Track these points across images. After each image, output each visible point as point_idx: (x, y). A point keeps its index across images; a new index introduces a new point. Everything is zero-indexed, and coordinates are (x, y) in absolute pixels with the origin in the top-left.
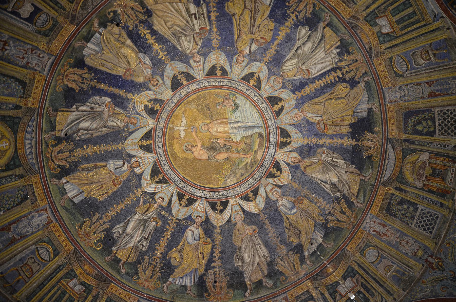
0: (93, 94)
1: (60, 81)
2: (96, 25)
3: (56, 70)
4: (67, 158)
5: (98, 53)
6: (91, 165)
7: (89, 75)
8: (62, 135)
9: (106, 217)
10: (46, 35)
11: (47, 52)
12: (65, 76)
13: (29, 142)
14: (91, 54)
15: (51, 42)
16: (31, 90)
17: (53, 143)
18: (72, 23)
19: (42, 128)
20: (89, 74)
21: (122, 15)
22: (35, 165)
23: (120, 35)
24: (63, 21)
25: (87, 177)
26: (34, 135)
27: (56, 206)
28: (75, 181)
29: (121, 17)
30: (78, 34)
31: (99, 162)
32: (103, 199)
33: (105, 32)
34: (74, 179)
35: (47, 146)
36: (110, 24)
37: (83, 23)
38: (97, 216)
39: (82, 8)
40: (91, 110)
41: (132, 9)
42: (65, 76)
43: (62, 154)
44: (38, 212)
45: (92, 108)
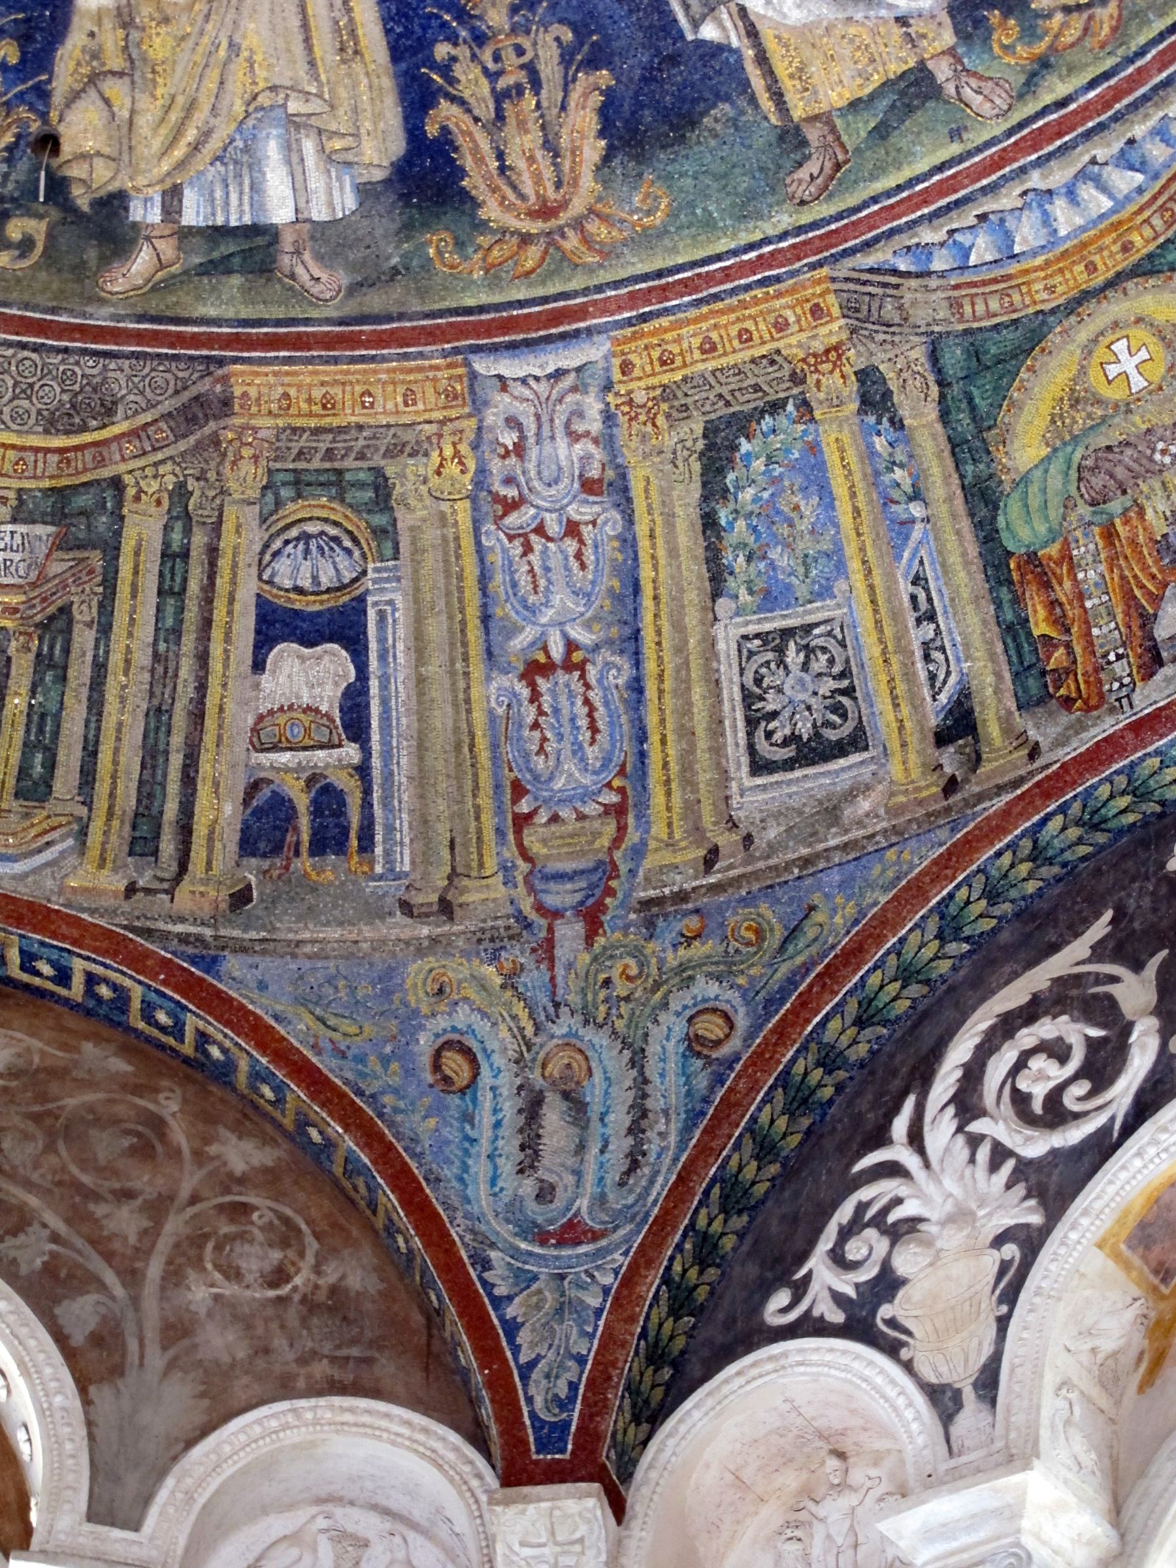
2: (141, 263)
3: (545, 300)
5: (294, 123)
7: (458, 71)
11: (473, 423)
13: (1059, 208)
14: (328, 158)
15: (409, 436)
18: (227, 402)
19: (940, 168)
20: (452, 81)
23: (93, 79)
24: (247, 452)
26: (1008, 199)
33: (141, 181)
35: (1044, 64)
36: (77, 191)
39: (108, 411)
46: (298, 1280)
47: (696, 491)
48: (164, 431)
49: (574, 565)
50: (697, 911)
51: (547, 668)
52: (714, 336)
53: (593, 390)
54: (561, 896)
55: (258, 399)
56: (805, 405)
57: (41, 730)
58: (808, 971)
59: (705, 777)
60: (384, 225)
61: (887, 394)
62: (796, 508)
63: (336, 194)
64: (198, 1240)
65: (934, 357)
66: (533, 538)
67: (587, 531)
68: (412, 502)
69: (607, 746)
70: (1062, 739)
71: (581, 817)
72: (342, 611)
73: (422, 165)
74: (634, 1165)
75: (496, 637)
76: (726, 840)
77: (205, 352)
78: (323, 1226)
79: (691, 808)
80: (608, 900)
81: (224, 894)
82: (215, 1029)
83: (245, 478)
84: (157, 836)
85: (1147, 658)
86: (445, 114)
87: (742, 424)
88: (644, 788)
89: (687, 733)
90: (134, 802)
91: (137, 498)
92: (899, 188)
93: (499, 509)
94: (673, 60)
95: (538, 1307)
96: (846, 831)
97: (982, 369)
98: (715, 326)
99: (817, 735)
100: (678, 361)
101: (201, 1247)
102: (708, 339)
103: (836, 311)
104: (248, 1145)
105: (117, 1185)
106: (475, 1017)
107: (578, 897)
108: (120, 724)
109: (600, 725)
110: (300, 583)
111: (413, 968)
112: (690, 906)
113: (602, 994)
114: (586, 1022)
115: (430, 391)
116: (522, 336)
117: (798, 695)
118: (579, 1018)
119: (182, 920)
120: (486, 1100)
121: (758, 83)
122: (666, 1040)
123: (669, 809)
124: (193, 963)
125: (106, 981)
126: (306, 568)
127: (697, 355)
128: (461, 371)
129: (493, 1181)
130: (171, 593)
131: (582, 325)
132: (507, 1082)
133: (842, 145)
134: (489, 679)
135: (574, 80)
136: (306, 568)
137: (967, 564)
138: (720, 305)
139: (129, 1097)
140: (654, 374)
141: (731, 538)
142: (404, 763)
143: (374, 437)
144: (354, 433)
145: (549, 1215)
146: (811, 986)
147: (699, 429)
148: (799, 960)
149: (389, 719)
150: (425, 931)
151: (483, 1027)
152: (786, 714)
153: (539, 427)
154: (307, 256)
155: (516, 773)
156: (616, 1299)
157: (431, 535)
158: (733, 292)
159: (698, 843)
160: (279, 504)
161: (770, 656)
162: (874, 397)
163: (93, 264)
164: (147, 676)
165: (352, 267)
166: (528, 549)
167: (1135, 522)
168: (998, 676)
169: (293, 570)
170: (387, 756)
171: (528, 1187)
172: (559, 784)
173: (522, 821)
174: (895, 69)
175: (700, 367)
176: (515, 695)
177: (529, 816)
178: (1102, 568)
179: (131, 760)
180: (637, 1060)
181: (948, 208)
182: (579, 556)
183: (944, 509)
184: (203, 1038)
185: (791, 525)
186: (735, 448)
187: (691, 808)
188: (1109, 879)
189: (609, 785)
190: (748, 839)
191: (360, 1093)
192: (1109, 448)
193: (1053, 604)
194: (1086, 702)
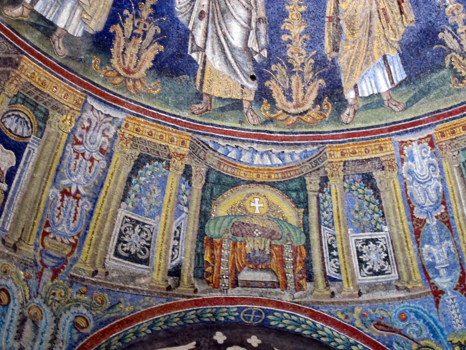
0: (171, 11)
1: (139, 87)
2: (17, 11)
3: (115, 94)
4: (303, 81)
6: (328, 29)
7: (127, 20)
8: (253, 86)
9: (454, 15)
10: (45, 118)
11: (79, 114)
12: (128, 76)
13: (257, 156)
14: (81, 18)
15: (61, 107)
16: (155, 144)
17: (266, 106)
18: (17, 65)
20: (124, 22)
22: (306, 151)
24: (15, 82)
25: (353, 42)
26: (245, 146)
27: (400, 122)
28: (357, 71)
31: (325, 8)
32: (412, 12)
34: (352, 71)
35: (271, 120)
38: (446, 36)
40: (205, 19)
42: (128, 76)
43: (294, 92)
44: (402, 160)
45: (201, 15)
47: (129, 170)
49: (88, 170)
50: (86, 286)
51: (69, 194)
52: (154, 132)
54: (49, 262)
55: (26, 70)
56: (168, 165)
58: (114, 320)
59: (101, 249)
60: (85, 45)
61: (191, 175)
62: (154, 190)
63: (78, 29)
65: (208, 173)
66: (80, 155)
67: (95, 162)
68: (52, 125)
69: (77, 226)
70: (204, 292)
71: (62, 242)
73: (103, 37)
75: (58, 177)
76: (100, 270)
77: (19, 47)
79: (94, 256)
80: (62, 270)
85: (234, 282)
86: (117, 28)
87: (150, 159)
89: (100, 234)
92: (220, 126)
93: (75, 142)
94: (181, 56)
96: (136, 285)
97: (219, 184)
98: (155, 130)
99: (136, 254)
100: (141, 133)
102: (151, 132)
103: (188, 146)
106: (13, 285)
107: (54, 264)
109: (77, 218)
110: (11, 128)
114: (45, 303)
115: (72, 98)
116: (104, 99)
117: (134, 241)
121: (199, 77)
122: (67, 319)
123: (88, 253)
126: (15, 125)
127: (146, 134)
128: (84, 98)
129: (7, 338)
131: (121, 107)
132: (17, 309)
133: (211, 106)
134: (51, 188)
135: (154, 43)
136: (15, 125)
137: (193, 231)
138: (159, 125)
142: (18, 198)
143: (51, 101)
144: (46, 96)
146: (115, 325)
147: (138, 153)
148: (113, 315)
149: (19, 183)
150: (7, 251)
151: (14, 289)
152: (129, 244)
153: (96, 126)
154: (61, 40)
155: (48, 219)
157: (53, 137)
158: (165, 124)
160: (16, 102)
161: (131, 226)
162: (187, 173)
165: (71, 51)
166: (77, 158)
167: (243, 246)
168: (191, 266)
170: (14, 193)
172: (60, 229)
173: (45, 234)
174: (234, 96)
176: (57, 197)
178: (230, 252)
180: (57, 321)
181: (229, 139)
182: (90, 168)
183: (193, 213)
185: (151, 194)
186: (145, 164)
187: (94, 256)
188: (195, 333)
189: (73, 237)
190: (107, 273)
192: (243, 223)
193: (212, 254)
194: (214, 285)
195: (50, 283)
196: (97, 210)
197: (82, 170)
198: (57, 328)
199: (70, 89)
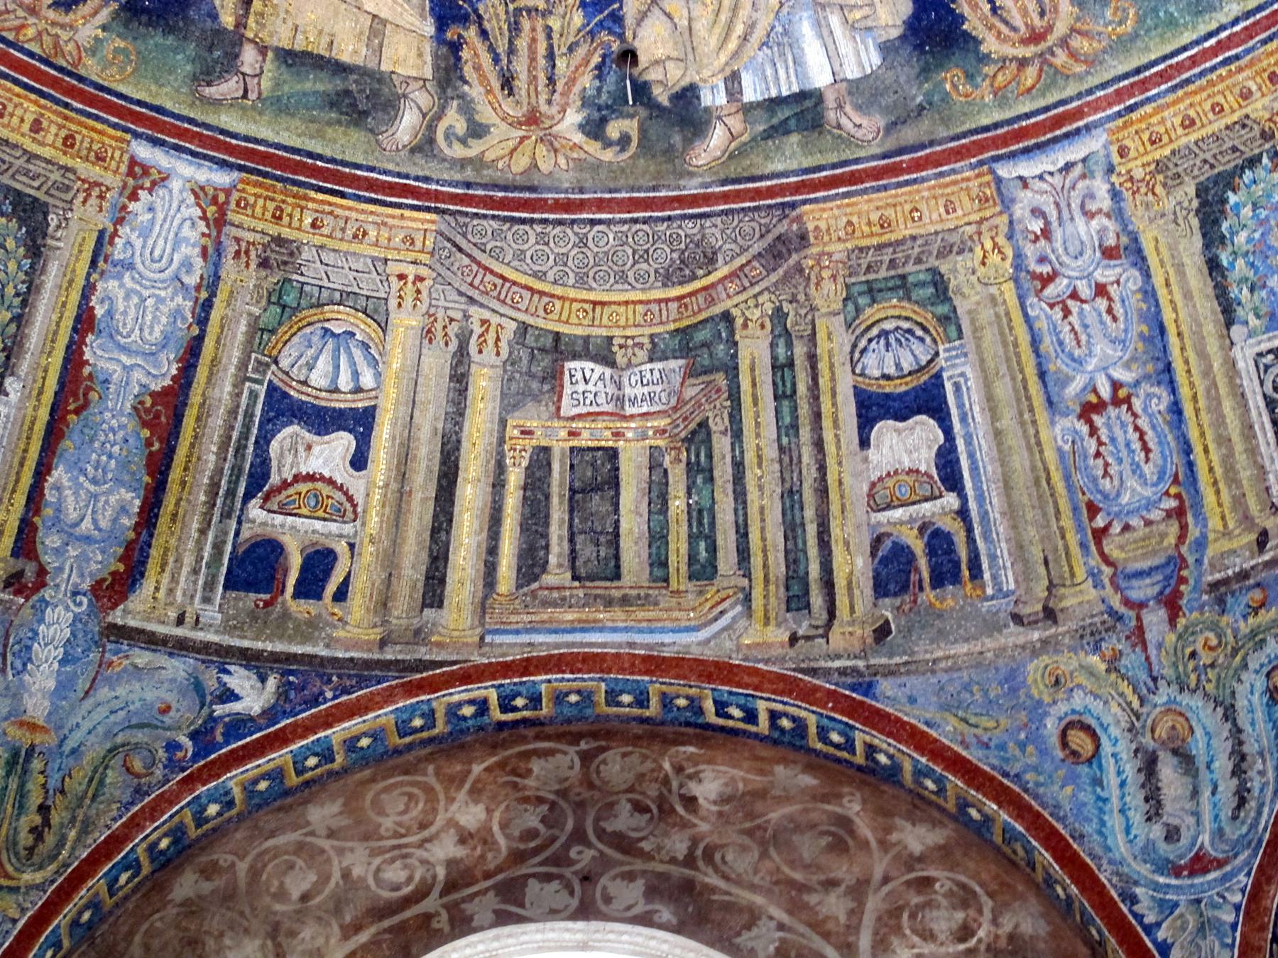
2: (717, 139)
3: (1047, 109)
11: (1004, 219)
14: (852, 27)
15: (954, 238)
16: (1217, 138)
18: (803, 237)
21: (577, 89)
29: (587, 81)
30: (820, 168)
33: (706, 73)
37: (758, 194)
39: (710, 260)
41: (508, 83)
42: (1043, 46)
46: (981, 933)
48: (757, 269)
49: (1108, 319)
50: (1258, 585)
51: (1099, 407)
52: (1192, 113)
53: (1099, 175)
54: (1143, 590)
57: (700, 523)
59: (1245, 474)
60: (905, 72)
63: (863, 54)
64: (895, 913)
66: (1070, 303)
67: (1113, 290)
68: (966, 290)
69: (1160, 462)
71: (1148, 523)
72: (924, 388)
74: (1242, 802)
77: (779, 200)
78: (994, 887)
79: (1239, 501)
80: (1183, 588)
81: (868, 631)
82: (879, 740)
83: (828, 295)
84: (807, 593)
87: (1228, 181)
88: (1197, 491)
90: (783, 569)
91: (745, 326)
93: (1038, 285)
95: (1183, 928)
100: (1165, 139)
101: (899, 917)
102: (1187, 117)
104: (921, 830)
105: (823, 877)
106: (1089, 699)
107: (1157, 589)
108: (762, 509)
109: (1151, 445)
110: (886, 371)
111: (1031, 667)
112: (1252, 581)
113: (1191, 665)
114: (1181, 690)
115: (966, 200)
116: (1033, 142)
118: (1175, 687)
119: (838, 657)
120: (1110, 765)
122: (1250, 693)
123: (1220, 505)
124: (853, 690)
125: (786, 715)
127: (1180, 131)
128: (988, 178)
129: (1127, 830)
130: (784, 396)
131: (1081, 123)
132: (1124, 748)
134: (1053, 423)
138: (1191, 87)
139: (820, 805)
140: (1146, 153)
141: (1233, 276)
143: (926, 243)
144: (909, 243)
145: (1180, 852)
147: (1192, 191)
149: (977, 468)
150: (1036, 635)
151: (1097, 706)
153: (1060, 212)
154: (848, 108)
156: (1247, 913)
157: (986, 315)
158: (1201, 74)
159: (1249, 529)
160: (858, 310)
163: (679, 146)
164: (777, 466)
165: (886, 110)
166: (1067, 312)
169: (878, 362)
170: (980, 498)
171: (1157, 831)
172: (1125, 499)
173: (1100, 534)
175: (1184, 140)
177: (1105, 530)
179: (776, 536)
180: (1229, 714)
182: (1110, 311)
184: (871, 749)
186: (1224, 201)
187: (1239, 501)
189: (1167, 493)
191: (1006, 775)
195: (1171, 638)
196: (1185, 392)
197: (1095, 330)
198: (1237, 730)
199: (947, 185)
